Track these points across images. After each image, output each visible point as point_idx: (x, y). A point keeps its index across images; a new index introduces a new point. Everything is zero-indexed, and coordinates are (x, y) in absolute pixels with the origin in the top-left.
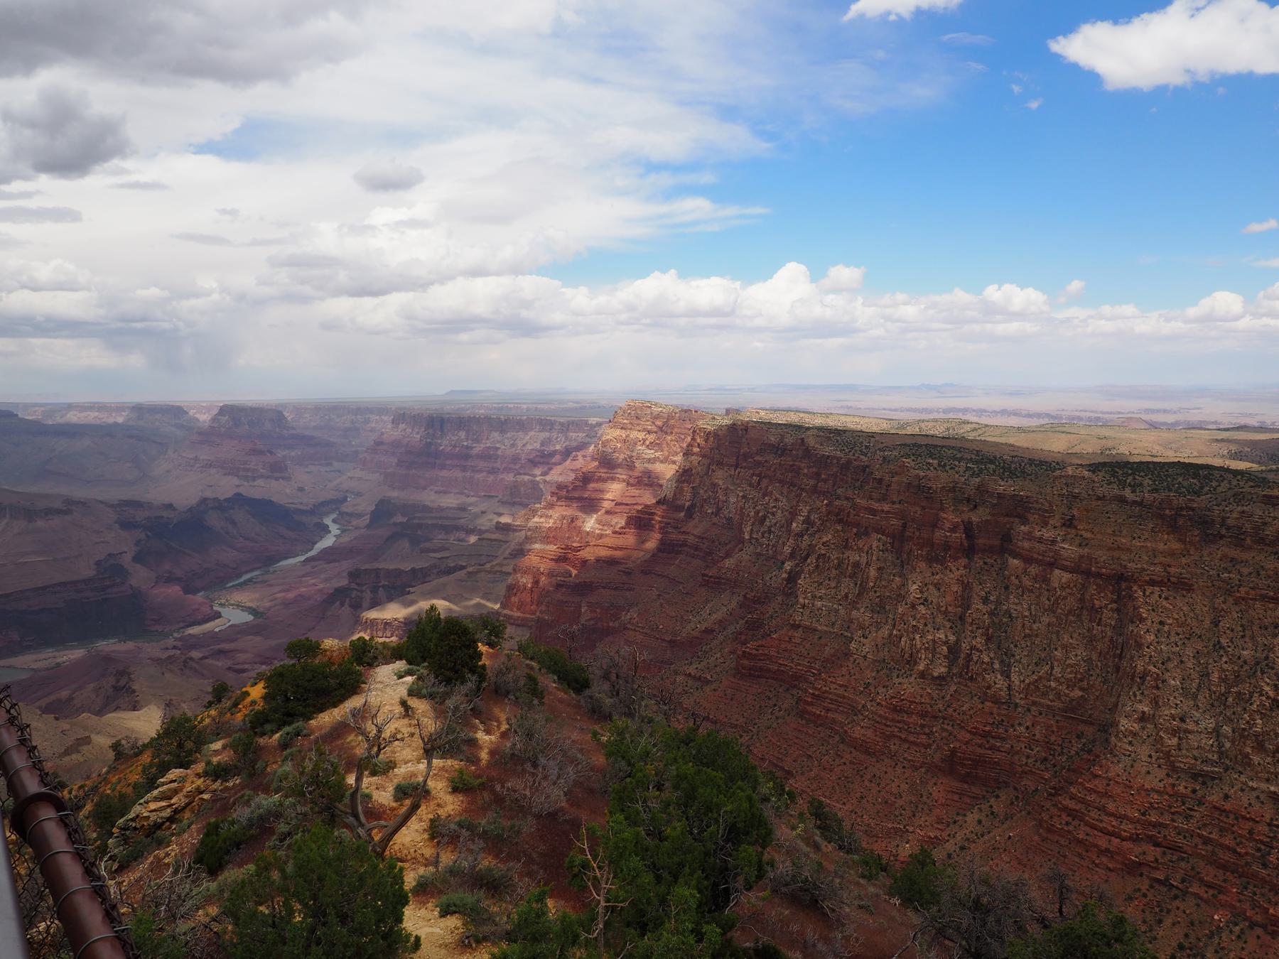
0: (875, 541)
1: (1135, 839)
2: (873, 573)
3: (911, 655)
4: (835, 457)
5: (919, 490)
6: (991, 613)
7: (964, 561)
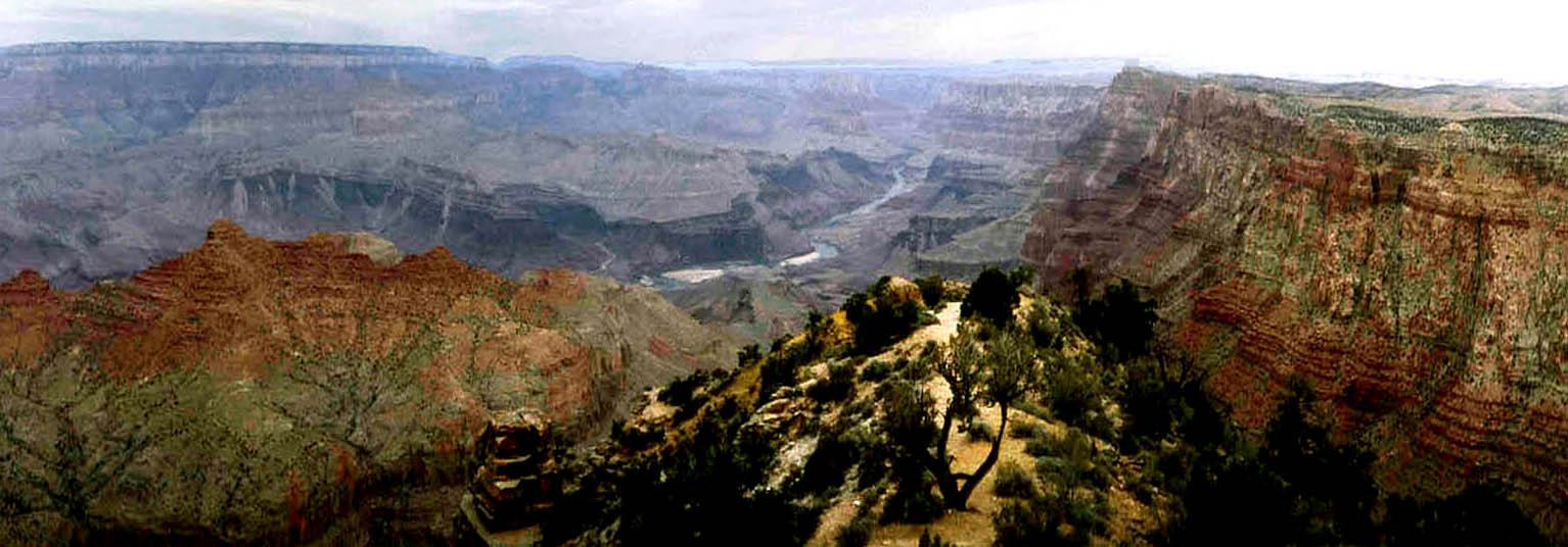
0: (1306, 195)
1: (1480, 446)
2: (1302, 225)
3: (1327, 298)
4: (1278, 118)
5: (1342, 149)
6: (1388, 257)
7: (1370, 210)
